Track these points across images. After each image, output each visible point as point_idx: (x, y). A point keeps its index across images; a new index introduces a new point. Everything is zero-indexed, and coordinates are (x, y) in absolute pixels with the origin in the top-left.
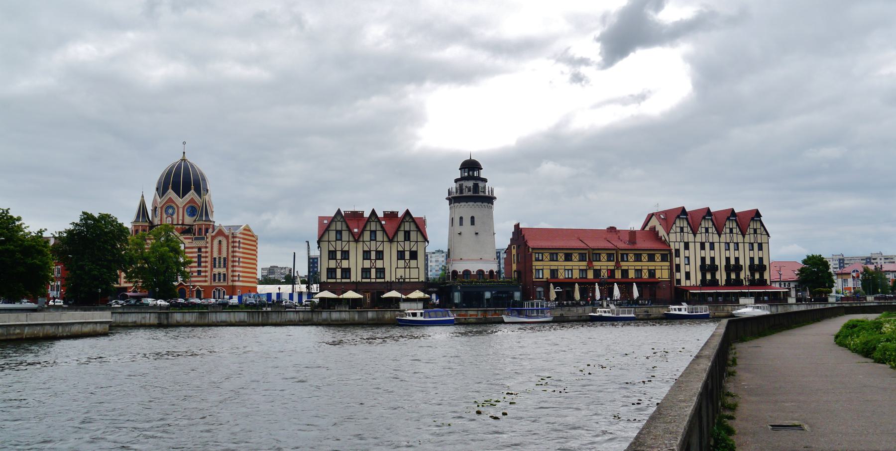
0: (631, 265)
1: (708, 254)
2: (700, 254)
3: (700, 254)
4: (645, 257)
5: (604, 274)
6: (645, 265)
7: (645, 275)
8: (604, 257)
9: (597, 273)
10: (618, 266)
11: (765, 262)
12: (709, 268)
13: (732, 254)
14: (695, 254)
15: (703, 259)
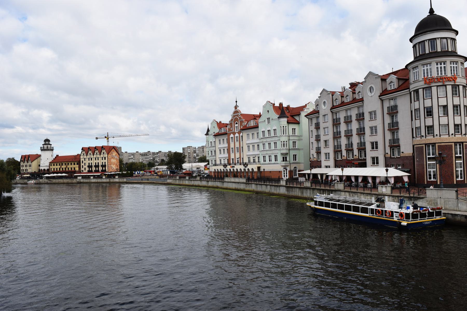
0: (70, 166)
1: (90, 162)
2: (88, 162)
3: (88, 162)
4: (73, 164)
5: (64, 169)
6: (73, 166)
7: (73, 169)
8: (64, 164)
9: (63, 169)
10: (67, 167)
11: (107, 164)
12: (90, 166)
13: (97, 161)
14: (87, 162)
15: (89, 163)
